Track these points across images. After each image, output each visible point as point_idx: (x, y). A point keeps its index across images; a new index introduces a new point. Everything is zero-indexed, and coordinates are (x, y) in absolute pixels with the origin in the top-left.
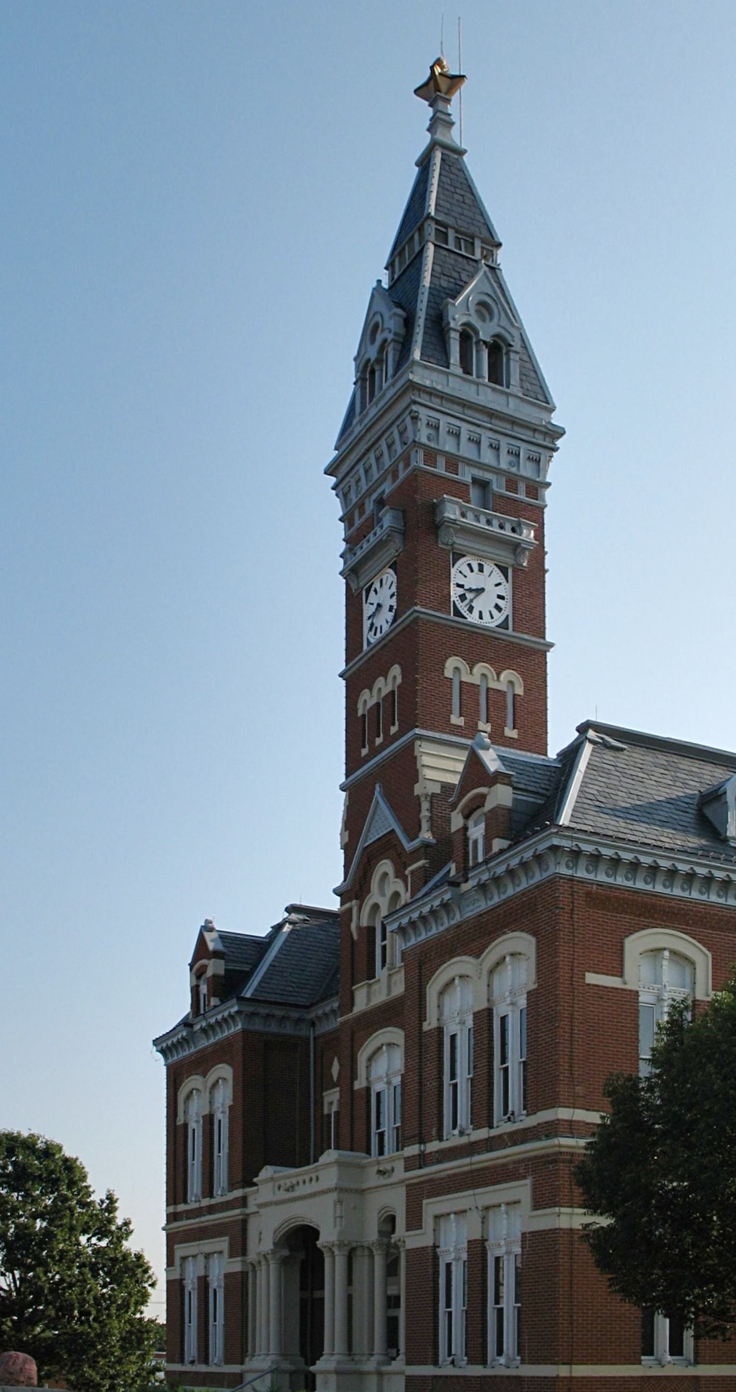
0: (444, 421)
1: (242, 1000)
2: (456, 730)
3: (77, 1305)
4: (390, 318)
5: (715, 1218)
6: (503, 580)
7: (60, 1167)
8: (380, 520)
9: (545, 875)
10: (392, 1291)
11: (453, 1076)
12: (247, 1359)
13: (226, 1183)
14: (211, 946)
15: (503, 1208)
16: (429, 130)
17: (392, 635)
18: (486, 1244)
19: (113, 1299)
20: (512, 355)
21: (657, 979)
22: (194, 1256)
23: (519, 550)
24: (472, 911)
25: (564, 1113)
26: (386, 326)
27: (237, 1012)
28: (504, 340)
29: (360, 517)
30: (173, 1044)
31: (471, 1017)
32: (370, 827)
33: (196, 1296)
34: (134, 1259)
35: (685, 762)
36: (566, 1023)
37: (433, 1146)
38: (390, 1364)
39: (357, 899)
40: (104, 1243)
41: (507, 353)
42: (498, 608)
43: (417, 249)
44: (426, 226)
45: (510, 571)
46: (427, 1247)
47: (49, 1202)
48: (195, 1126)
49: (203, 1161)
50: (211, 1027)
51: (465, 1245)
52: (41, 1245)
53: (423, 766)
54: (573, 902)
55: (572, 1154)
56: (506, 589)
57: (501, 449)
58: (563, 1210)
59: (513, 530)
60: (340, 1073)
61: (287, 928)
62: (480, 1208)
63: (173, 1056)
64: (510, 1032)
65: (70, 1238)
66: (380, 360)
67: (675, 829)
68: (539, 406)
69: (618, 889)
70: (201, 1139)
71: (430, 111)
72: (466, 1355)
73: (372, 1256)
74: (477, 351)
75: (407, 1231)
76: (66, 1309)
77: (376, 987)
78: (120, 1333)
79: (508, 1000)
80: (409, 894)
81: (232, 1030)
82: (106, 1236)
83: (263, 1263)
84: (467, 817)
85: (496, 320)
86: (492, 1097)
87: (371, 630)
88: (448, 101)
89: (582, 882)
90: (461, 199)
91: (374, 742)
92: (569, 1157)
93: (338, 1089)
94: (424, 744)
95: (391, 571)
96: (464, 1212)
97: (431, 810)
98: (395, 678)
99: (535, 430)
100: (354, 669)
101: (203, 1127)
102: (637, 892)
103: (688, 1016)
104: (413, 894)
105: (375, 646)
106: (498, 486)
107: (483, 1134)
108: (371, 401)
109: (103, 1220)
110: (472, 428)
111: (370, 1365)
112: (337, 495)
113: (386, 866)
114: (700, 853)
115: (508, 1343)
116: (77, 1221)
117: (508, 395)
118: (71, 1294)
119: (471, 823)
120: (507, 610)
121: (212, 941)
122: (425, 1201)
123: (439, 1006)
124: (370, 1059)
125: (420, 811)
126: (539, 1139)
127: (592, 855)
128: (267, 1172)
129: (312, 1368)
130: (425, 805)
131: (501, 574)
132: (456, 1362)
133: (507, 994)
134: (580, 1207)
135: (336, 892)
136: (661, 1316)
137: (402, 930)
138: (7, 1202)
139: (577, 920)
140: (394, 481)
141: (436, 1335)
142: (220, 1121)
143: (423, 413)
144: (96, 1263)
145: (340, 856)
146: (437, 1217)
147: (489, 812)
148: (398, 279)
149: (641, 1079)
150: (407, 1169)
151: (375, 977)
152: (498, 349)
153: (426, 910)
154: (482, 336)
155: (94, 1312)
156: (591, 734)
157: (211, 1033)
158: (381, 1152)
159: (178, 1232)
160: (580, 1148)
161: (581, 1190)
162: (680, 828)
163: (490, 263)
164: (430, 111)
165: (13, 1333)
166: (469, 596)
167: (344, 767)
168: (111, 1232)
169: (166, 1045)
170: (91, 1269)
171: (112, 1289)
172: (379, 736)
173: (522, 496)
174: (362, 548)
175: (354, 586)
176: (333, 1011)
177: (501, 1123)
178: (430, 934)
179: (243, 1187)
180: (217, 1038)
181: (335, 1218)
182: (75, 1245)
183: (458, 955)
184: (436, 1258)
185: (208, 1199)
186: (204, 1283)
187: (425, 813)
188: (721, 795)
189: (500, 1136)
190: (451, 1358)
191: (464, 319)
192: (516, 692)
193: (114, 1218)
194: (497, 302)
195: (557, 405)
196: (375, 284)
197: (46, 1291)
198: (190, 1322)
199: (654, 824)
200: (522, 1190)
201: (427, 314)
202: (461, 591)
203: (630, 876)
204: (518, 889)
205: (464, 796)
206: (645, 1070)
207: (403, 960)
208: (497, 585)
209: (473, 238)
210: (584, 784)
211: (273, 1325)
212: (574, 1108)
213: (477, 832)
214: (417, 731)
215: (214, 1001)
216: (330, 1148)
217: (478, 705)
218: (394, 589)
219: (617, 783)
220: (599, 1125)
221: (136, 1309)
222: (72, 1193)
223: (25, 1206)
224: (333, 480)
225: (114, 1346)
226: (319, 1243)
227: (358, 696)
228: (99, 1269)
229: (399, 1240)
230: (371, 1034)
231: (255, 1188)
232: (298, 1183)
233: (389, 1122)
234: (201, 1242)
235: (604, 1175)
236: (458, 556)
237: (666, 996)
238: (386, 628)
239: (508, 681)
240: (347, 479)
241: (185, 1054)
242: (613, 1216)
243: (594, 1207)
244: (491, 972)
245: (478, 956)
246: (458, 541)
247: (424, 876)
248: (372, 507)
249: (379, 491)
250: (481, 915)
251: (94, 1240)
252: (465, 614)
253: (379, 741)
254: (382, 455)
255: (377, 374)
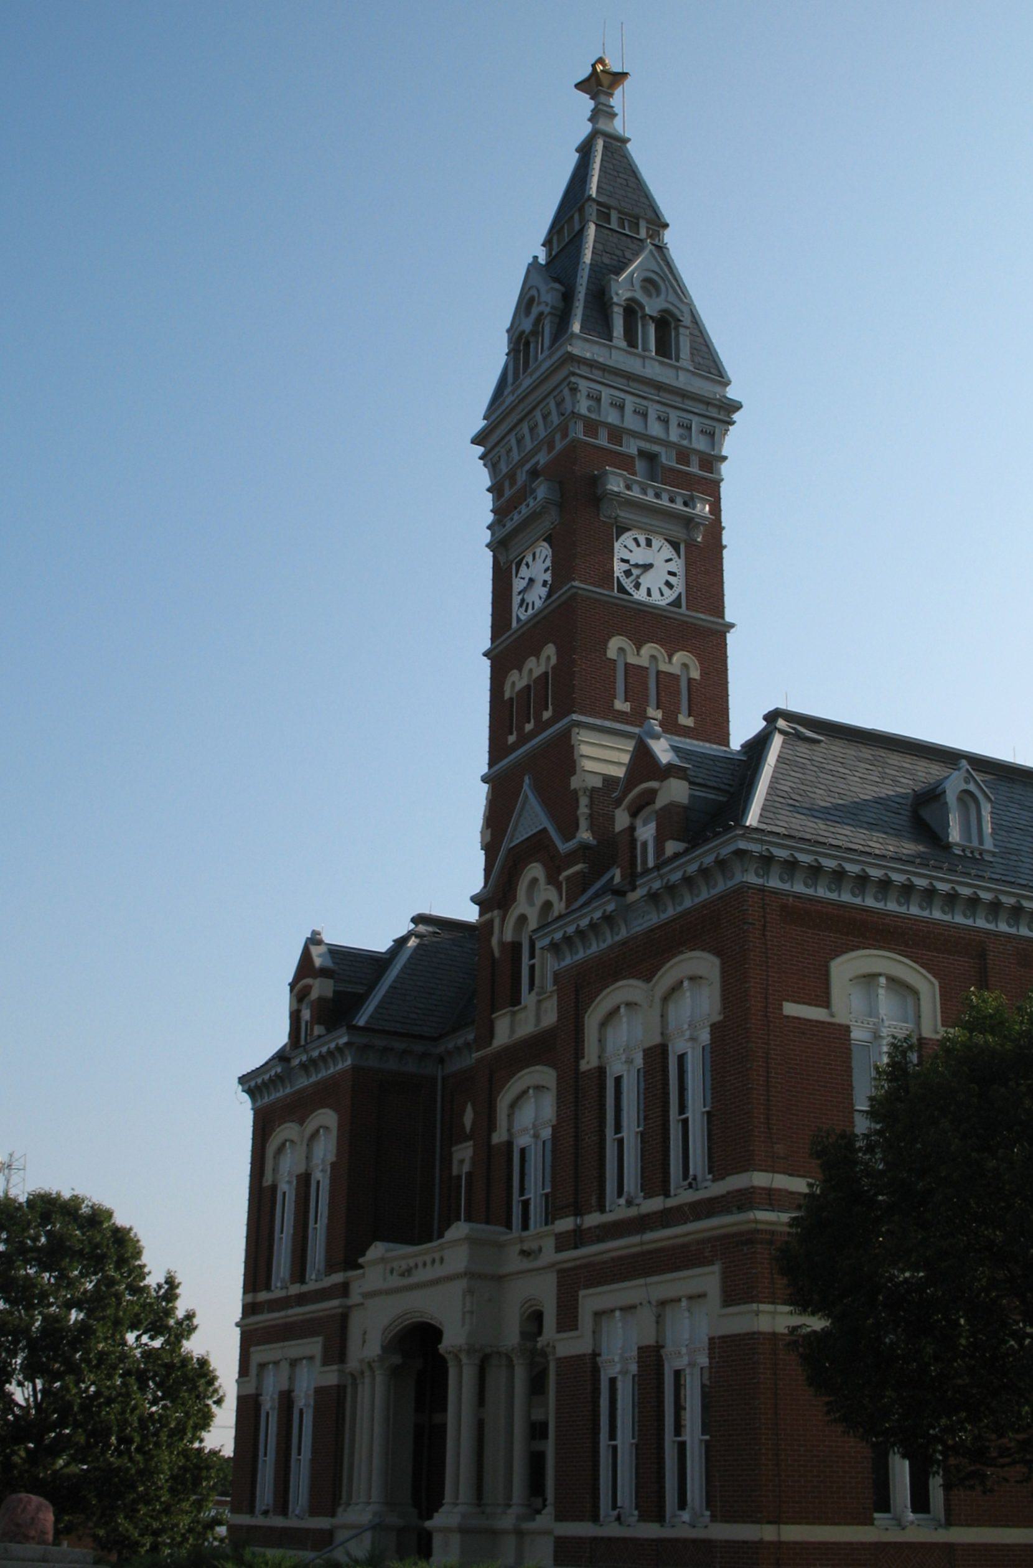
0: (606, 393)
1: (353, 1029)
2: (620, 717)
3: (115, 1428)
4: (548, 292)
5: (962, 1321)
6: (675, 556)
7: (108, 1239)
8: (533, 491)
9: (730, 884)
10: (537, 1415)
11: (618, 1128)
12: (340, 1510)
13: (323, 1264)
14: (318, 962)
15: (684, 1303)
16: (590, 120)
17: (546, 612)
18: (663, 1352)
19: (164, 1421)
20: (682, 330)
21: (872, 1012)
22: (276, 1363)
23: (692, 525)
24: (641, 925)
25: (760, 1179)
26: (543, 299)
27: (346, 1044)
28: (672, 315)
29: (511, 488)
30: (263, 1082)
31: (641, 1054)
32: (517, 825)
33: (275, 1419)
34: (196, 1366)
35: (894, 757)
36: (762, 1068)
37: (593, 1220)
38: (534, 1520)
39: (499, 908)
40: (157, 1343)
41: (676, 328)
42: (669, 584)
43: (577, 228)
44: (586, 206)
45: (682, 547)
46: (584, 1355)
47: (89, 1286)
48: (287, 1188)
49: (294, 1235)
50: (313, 1062)
51: (635, 1353)
52: (74, 1345)
53: (582, 756)
54: (764, 917)
55: (773, 1233)
56: (678, 565)
57: (670, 422)
58: (762, 1307)
59: (686, 504)
60: (474, 1123)
61: (412, 942)
62: (654, 1303)
63: (262, 1098)
64: (690, 1075)
65: (113, 1335)
66: (536, 332)
67: (885, 833)
68: (713, 380)
69: (819, 902)
70: (293, 1205)
71: (591, 104)
72: (636, 1508)
73: (511, 1366)
74: (643, 326)
75: (558, 1332)
76: (100, 1434)
77: (521, 1016)
78: (171, 1469)
79: (688, 1033)
80: (563, 904)
81: (340, 1066)
82: (162, 1334)
83: (367, 1373)
84: (634, 814)
85: (663, 296)
86: (669, 1156)
87: (521, 605)
88: (611, 95)
89: (775, 893)
90: (624, 182)
91: (523, 728)
92: (768, 1237)
93: (471, 1143)
94: (583, 732)
95: (545, 544)
96: (633, 1307)
97: (591, 805)
98: (548, 658)
99: (708, 404)
100: (501, 648)
101: (297, 1189)
102: (843, 906)
103: (914, 1057)
104: (569, 903)
105: (526, 623)
106: (667, 459)
107: (655, 1204)
108: (524, 372)
109: (160, 1312)
110: (638, 400)
111: (507, 1521)
112: (485, 465)
113: (535, 870)
114: (918, 861)
115: (693, 1492)
116: (124, 1313)
117: (677, 368)
118: (108, 1413)
119: (639, 822)
120: (679, 583)
121: (320, 956)
122: (582, 1293)
123: (600, 1041)
124: (513, 1105)
125: (578, 807)
126: (729, 1212)
127: (786, 861)
128: (377, 1250)
129: (428, 1524)
130: (584, 801)
131: (671, 549)
132: (622, 1519)
133: (686, 1026)
134: (784, 1303)
135: (475, 899)
136: (897, 1457)
137: (554, 947)
138: (34, 1286)
139: (769, 936)
140: (549, 452)
141: (596, 1478)
142: (318, 1182)
143: (583, 385)
144: (146, 1370)
145: (480, 857)
146: (598, 1315)
147: (661, 809)
148: (556, 255)
149: (857, 1136)
150: (559, 1249)
151: (520, 1003)
152: (666, 324)
153: (584, 923)
154: (648, 311)
155: (137, 1439)
156: (781, 723)
157: (312, 1069)
158: (525, 1226)
159: (256, 1330)
160: (782, 1224)
161: (785, 1281)
162: (892, 831)
163: (656, 242)
164: (591, 104)
165: (27, 1467)
166: (636, 572)
167: (486, 756)
168: (169, 1329)
169: (254, 1084)
170: (138, 1379)
171: (165, 1407)
172: (529, 722)
173: (694, 469)
174: (512, 519)
175: (502, 560)
176: (468, 1045)
177: (680, 1191)
178: (589, 952)
179: (345, 1270)
180: (320, 1076)
181: (464, 1313)
182: (120, 1344)
183: (624, 978)
184: (596, 1370)
185: (298, 1285)
186: (286, 1400)
187: (583, 810)
188: (939, 795)
189: (679, 1208)
190: (616, 1513)
191: (628, 295)
192: (692, 676)
193: (174, 1308)
194: (664, 277)
195: (732, 379)
196: (530, 260)
197: (76, 1409)
198: (265, 1455)
199: (861, 827)
200: (708, 1279)
201: (587, 289)
202: (625, 566)
203: (833, 886)
204: (697, 900)
205: (630, 791)
206: (862, 1125)
207: (555, 982)
208: (667, 561)
209: (638, 219)
210: (774, 780)
211: (377, 1462)
212: (774, 1172)
213: (646, 832)
214: (575, 717)
215: (318, 1030)
216: (459, 1220)
217: (647, 689)
218: (548, 563)
219: (814, 779)
220: (805, 1195)
221: (194, 1435)
222: (121, 1274)
223: (58, 1290)
224: (480, 450)
225: (161, 1488)
226: (442, 1348)
227: (505, 677)
228: (149, 1379)
229: (548, 1345)
230: (514, 1074)
231: (360, 1271)
232: (416, 1266)
233: (536, 1188)
234: (286, 1343)
235: (810, 1263)
236: (622, 530)
237: (884, 1032)
238: (538, 604)
239: (682, 663)
240: (497, 449)
241: (278, 1095)
242: (829, 1316)
243: (802, 1303)
244: (665, 999)
245: (648, 980)
246: (622, 514)
247: (581, 884)
248: (524, 478)
249: (533, 461)
250: (652, 930)
251: (145, 1339)
252: (631, 591)
253: (529, 727)
254: (536, 425)
255: (532, 346)
